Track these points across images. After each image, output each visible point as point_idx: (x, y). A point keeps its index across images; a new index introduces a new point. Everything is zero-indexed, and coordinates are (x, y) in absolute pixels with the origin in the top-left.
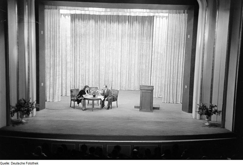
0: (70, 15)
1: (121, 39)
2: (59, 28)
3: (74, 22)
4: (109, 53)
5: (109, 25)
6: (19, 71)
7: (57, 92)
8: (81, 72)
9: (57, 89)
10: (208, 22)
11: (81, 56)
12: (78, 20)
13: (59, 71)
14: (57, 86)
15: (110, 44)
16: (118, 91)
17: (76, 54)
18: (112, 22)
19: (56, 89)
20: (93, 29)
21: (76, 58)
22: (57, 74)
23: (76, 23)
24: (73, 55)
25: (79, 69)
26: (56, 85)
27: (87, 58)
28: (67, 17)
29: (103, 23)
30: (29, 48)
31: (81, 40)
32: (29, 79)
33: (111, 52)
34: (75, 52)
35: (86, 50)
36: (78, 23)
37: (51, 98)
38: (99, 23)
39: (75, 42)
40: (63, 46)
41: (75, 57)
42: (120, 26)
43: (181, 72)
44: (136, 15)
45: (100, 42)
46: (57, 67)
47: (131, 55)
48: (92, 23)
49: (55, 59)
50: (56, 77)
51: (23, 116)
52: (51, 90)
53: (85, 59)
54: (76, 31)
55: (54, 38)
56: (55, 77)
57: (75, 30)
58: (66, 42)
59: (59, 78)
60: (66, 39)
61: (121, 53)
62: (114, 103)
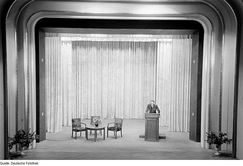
0: (71, 42)
1: (123, 66)
2: (60, 56)
3: (76, 49)
4: (111, 80)
5: (112, 51)
6: (18, 100)
8: (82, 101)
9: (58, 119)
10: (214, 45)
11: (83, 84)
12: (79, 48)
13: (60, 100)
14: (58, 116)
15: (113, 71)
16: (122, 120)
17: (78, 82)
18: (115, 48)
19: (57, 118)
20: (95, 56)
21: (78, 87)
22: (58, 103)
23: (77, 50)
25: (81, 97)
26: (57, 116)
27: (89, 86)
28: (68, 44)
29: (105, 50)
30: (28, 77)
31: (82, 68)
32: (28, 109)
33: (114, 80)
34: (76, 80)
35: (88, 77)
36: (79, 51)
37: (52, 128)
38: (101, 50)
39: (76, 70)
40: (64, 74)
41: (76, 85)
42: (123, 52)
43: (188, 63)
45: (103, 70)
46: (58, 96)
47: (134, 82)
48: (94, 50)
49: (56, 87)
50: (57, 105)
51: (23, 148)
52: (52, 119)
53: (87, 87)
54: (78, 58)
55: (55, 65)
56: (56, 107)
57: (76, 57)
59: (60, 107)
62: (119, 133)
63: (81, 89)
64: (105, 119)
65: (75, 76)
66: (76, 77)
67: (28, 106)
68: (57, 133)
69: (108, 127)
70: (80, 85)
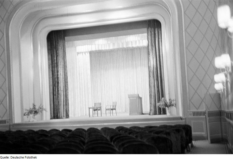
7: (77, 108)
16: (116, 103)
28: (86, 53)
30: (42, 70)
32: (42, 92)
41: (101, 88)
62: (114, 111)
64: (124, 112)
65: (100, 80)
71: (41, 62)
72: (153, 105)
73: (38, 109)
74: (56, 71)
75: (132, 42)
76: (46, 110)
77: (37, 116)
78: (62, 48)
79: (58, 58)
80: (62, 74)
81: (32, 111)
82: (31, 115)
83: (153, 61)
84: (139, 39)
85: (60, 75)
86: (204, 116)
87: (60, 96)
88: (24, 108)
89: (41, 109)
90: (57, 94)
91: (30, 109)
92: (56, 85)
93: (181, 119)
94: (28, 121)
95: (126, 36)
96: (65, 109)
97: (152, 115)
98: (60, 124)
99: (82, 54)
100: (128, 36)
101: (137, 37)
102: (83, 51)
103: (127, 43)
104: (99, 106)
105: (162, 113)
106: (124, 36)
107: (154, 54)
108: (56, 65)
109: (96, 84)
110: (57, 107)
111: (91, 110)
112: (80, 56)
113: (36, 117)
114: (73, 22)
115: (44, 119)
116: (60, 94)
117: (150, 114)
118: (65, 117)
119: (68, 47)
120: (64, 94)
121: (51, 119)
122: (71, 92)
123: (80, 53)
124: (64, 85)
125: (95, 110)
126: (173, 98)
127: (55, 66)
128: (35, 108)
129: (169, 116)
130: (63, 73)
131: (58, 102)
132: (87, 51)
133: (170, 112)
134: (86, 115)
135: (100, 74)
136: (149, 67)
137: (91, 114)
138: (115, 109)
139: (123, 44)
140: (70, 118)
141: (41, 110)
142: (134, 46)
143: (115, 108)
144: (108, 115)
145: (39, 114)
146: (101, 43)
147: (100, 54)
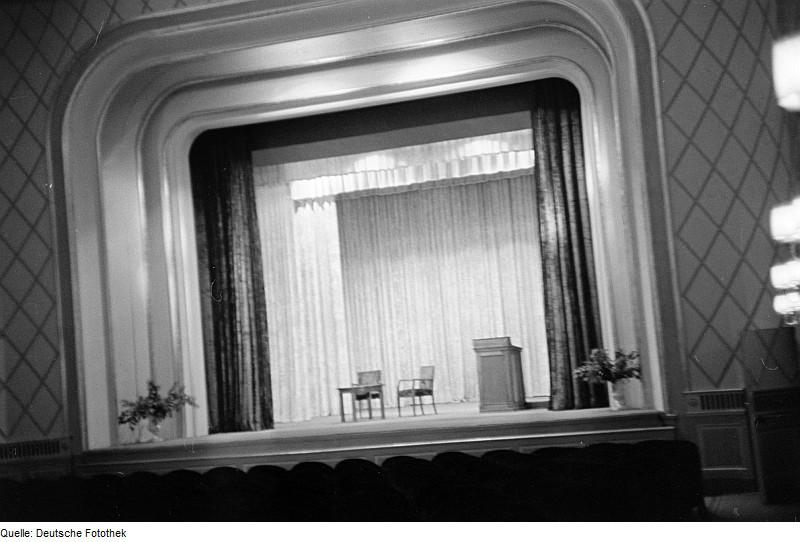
0: (333, 198)
2: (291, 232)
7: (298, 393)
8: (398, 358)
9: (298, 387)
13: (300, 340)
14: (298, 380)
16: (433, 368)
22: (296, 347)
24: (375, 310)
27: (410, 316)
28: (326, 204)
30: (175, 266)
31: (390, 271)
32: (180, 342)
37: (285, 413)
41: (379, 318)
44: (496, 171)
50: (293, 353)
51: (156, 424)
55: (281, 255)
56: (291, 357)
58: (330, 270)
59: (301, 357)
60: (329, 261)
61: (501, 290)
62: (427, 399)
63: (391, 326)
64: (462, 401)
65: (374, 293)
66: (377, 295)
67: (179, 333)
68: (299, 423)
69: (398, 388)
70: (387, 315)
71: (173, 237)
72: (560, 376)
73: (167, 401)
74: (224, 269)
75: (479, 159)
76: (192, 404)
77: (166, 424)
78: (243, 191)
79: (229, 223)
80: (244, 276)
81: (146, 407)
82: (145, 422)
83: (554, 221)
84: (505, 147)
85: (237, 281)
86: (742, 410)
87: (240, 353)
88: (121, 396)
89: (178, 399)
90: (229, 347)
91: (141, 398)
92: (226, 316)
93: (659, 418)
94: (133, 441)
95: (460, 140)
96: (258, 398)
97: (560, 409)
98: (242, 447)
99: (312, 205)
100: (468, 139)
101: (496, 143)
102: (313, 196)
103: (464, 163)
104: (376, 384)
105: (593, 400)
106: (452, 142)
107: (557, 200)
108: (223, 247)
109: (361, 307)
110: (231, 391)
111: (348, 397)
112: (305, 212)
113: (159, 426)
114: (278, 98)
115: (189, 433)
116: (240, 347)
117: (551, 408)
118: (258, 425)
119: (263, 185)
120: (252, 346)
121: (212, 432)
122: (278, 336)
123: (305, 201)
124: (253, 315)
125: (360, 398)
126: (630, 348)
127: (219, 249)
128: (155, 395)
129: (620, 410)
130: (249, 273)
131: (235, 374)
132: (327, 193)
133: (621, 398)
134: (330, 415)
135: (375, 272)
136: (543, 245)
137: (348, 410)
138: (430, 392)
139: (449, 166)
140: (275, 426)
141: (176, 402)
142: (488, 170)
143: (427, 387)
144: (407, 412)
145: (171, 416)
146: (376, 168)
147: (372, 204)
